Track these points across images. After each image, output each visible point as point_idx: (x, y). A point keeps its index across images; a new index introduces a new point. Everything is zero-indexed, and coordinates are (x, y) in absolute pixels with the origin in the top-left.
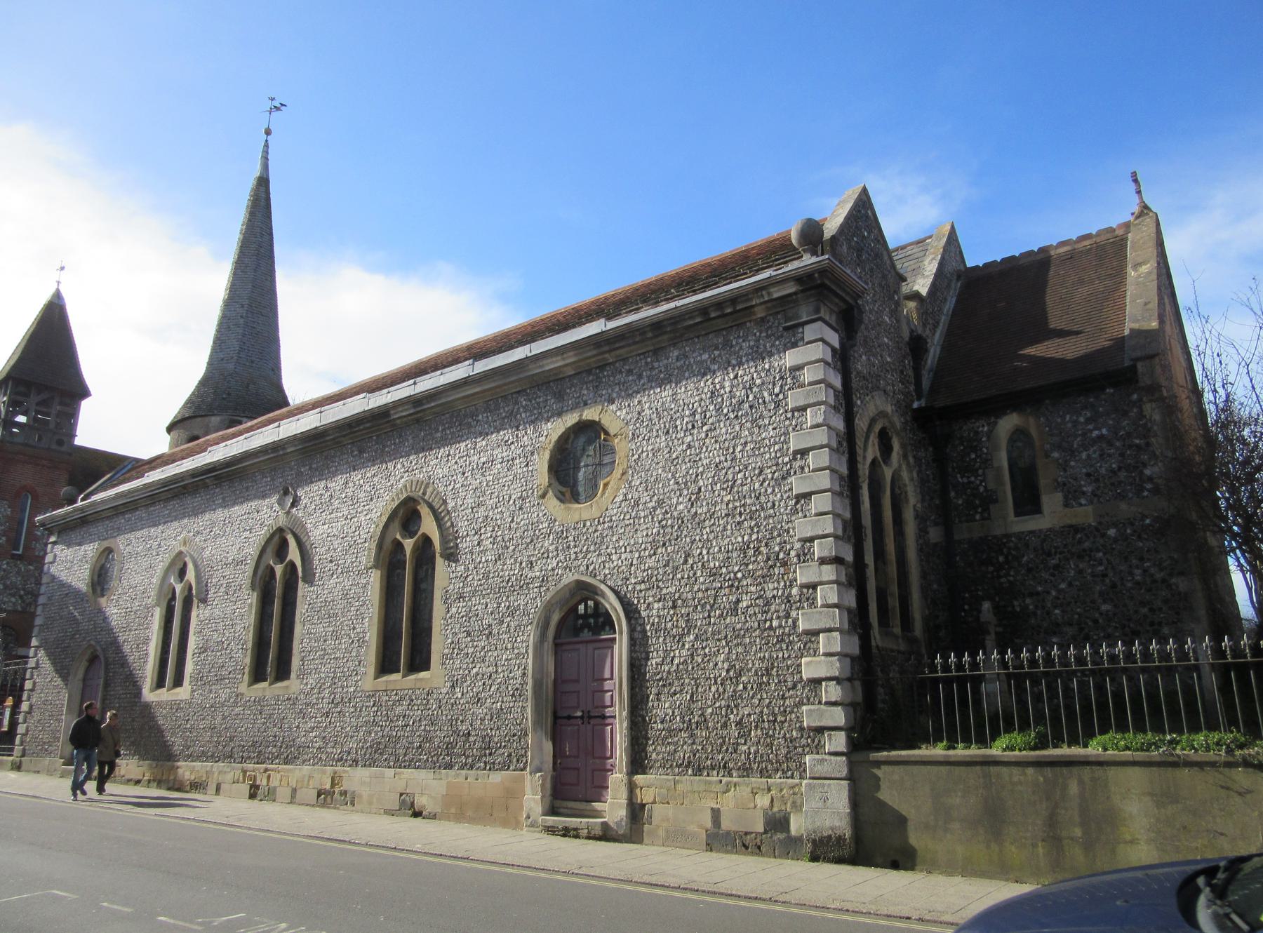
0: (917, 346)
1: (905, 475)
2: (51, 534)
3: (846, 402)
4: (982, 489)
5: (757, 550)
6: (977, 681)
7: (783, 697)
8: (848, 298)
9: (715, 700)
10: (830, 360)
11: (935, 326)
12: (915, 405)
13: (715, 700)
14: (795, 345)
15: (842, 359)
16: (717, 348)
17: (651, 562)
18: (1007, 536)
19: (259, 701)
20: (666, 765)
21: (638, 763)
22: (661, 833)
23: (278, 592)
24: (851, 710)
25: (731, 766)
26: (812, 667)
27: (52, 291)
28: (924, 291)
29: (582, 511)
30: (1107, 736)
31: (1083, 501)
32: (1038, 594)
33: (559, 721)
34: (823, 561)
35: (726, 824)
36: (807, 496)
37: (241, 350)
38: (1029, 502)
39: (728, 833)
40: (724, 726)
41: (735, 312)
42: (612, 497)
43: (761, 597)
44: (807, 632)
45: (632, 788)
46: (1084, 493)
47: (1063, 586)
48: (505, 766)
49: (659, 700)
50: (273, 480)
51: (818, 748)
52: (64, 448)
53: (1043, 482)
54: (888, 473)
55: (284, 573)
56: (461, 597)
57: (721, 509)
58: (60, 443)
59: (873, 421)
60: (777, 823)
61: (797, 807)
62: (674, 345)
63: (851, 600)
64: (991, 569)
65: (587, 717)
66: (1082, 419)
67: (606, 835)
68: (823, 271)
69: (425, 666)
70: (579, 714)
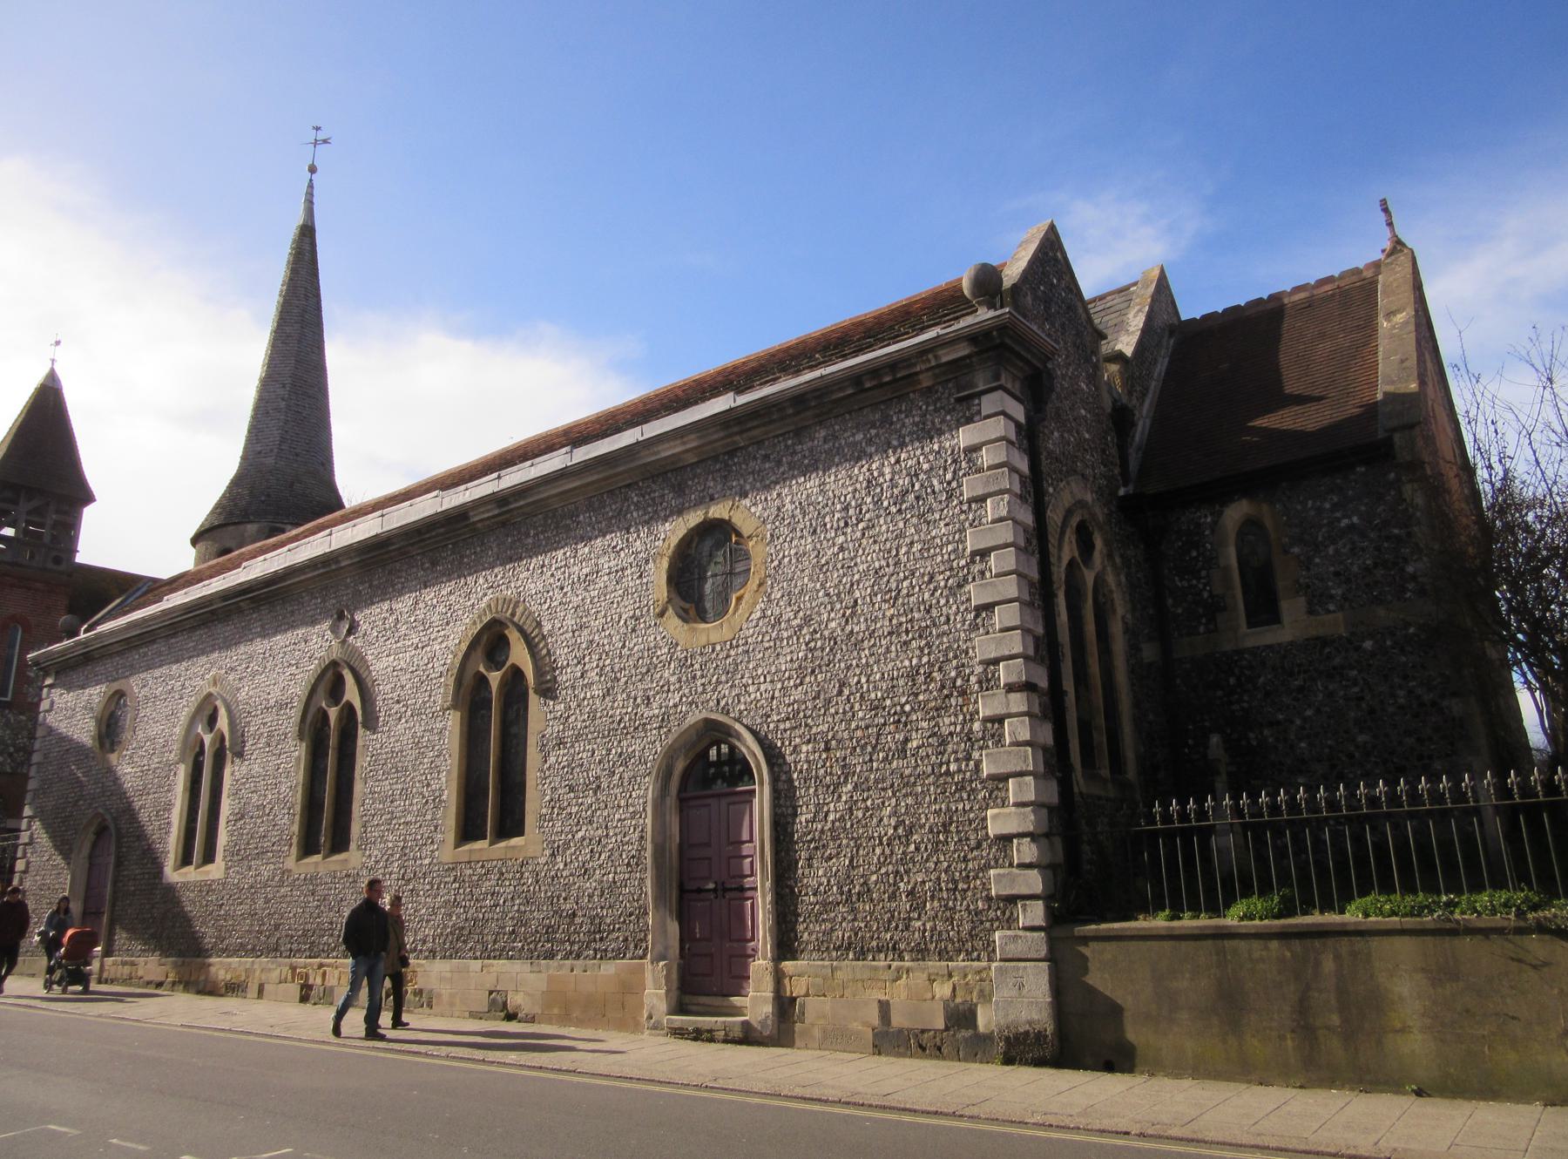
0: (1121, 419)
1: (1111, 579)
2: (47, 675)
3: (1034, 490)
4: (1206, 595)
5: (929, 676)
6: (1206, 833)
7: (965, 860)
8: (1035, 362)
9: (881, 865)
10: (1013, 438)
11: (1144, 395)
12: (1122, 492)
13: (881, 865)
14: (969, 420)
15: (1028, 437)
16: (873, 426)
17: (797, 694)
18: (1239, 652)
19: (312, 879)
20: (822, 948)
21: (786, 947)
22: (817, 1033)
23: (333, 741)
24: (1049, 873)
25: (902, 946)
26: (999, 821)
27: (46, 370)
28: (1129, 352)
29: (710, 632)
30: (1368, 899)
31: (1332, 607)
32: (1278, 723)
34: (1010, 688)
35: (898, 1020)
36: (989, 607)
37: (283, 440)
38: (1264, 609)
39: (900, 1031)
40: (893, 897)
41: (895, 380)
42: (747, 615)
43: (934, 734)
44: (992, 777)
45: (779, 977)
46: (1332, 597)
47: (1309, 713)
48: (619, 954)
49: (810, 866)
50: (324, 601)
51: (1010, 922)
52: (62, 567)
53: (1281, 584)
54: (1089, 577)
55: (340, 718)
56: (561, 743)
57: (883, 626)
58: (57, 561)
59: (1069, 513)
60: (961, 1017)
61: (986, 997)
62: (820, 423)
63: (1047, 735)
64: (1220, 693)
65: (721, 890)
66: (1327, 506)
67: (748, 1037)
68: (1002, 328)
69: (519, 831)
70: (711, 886)
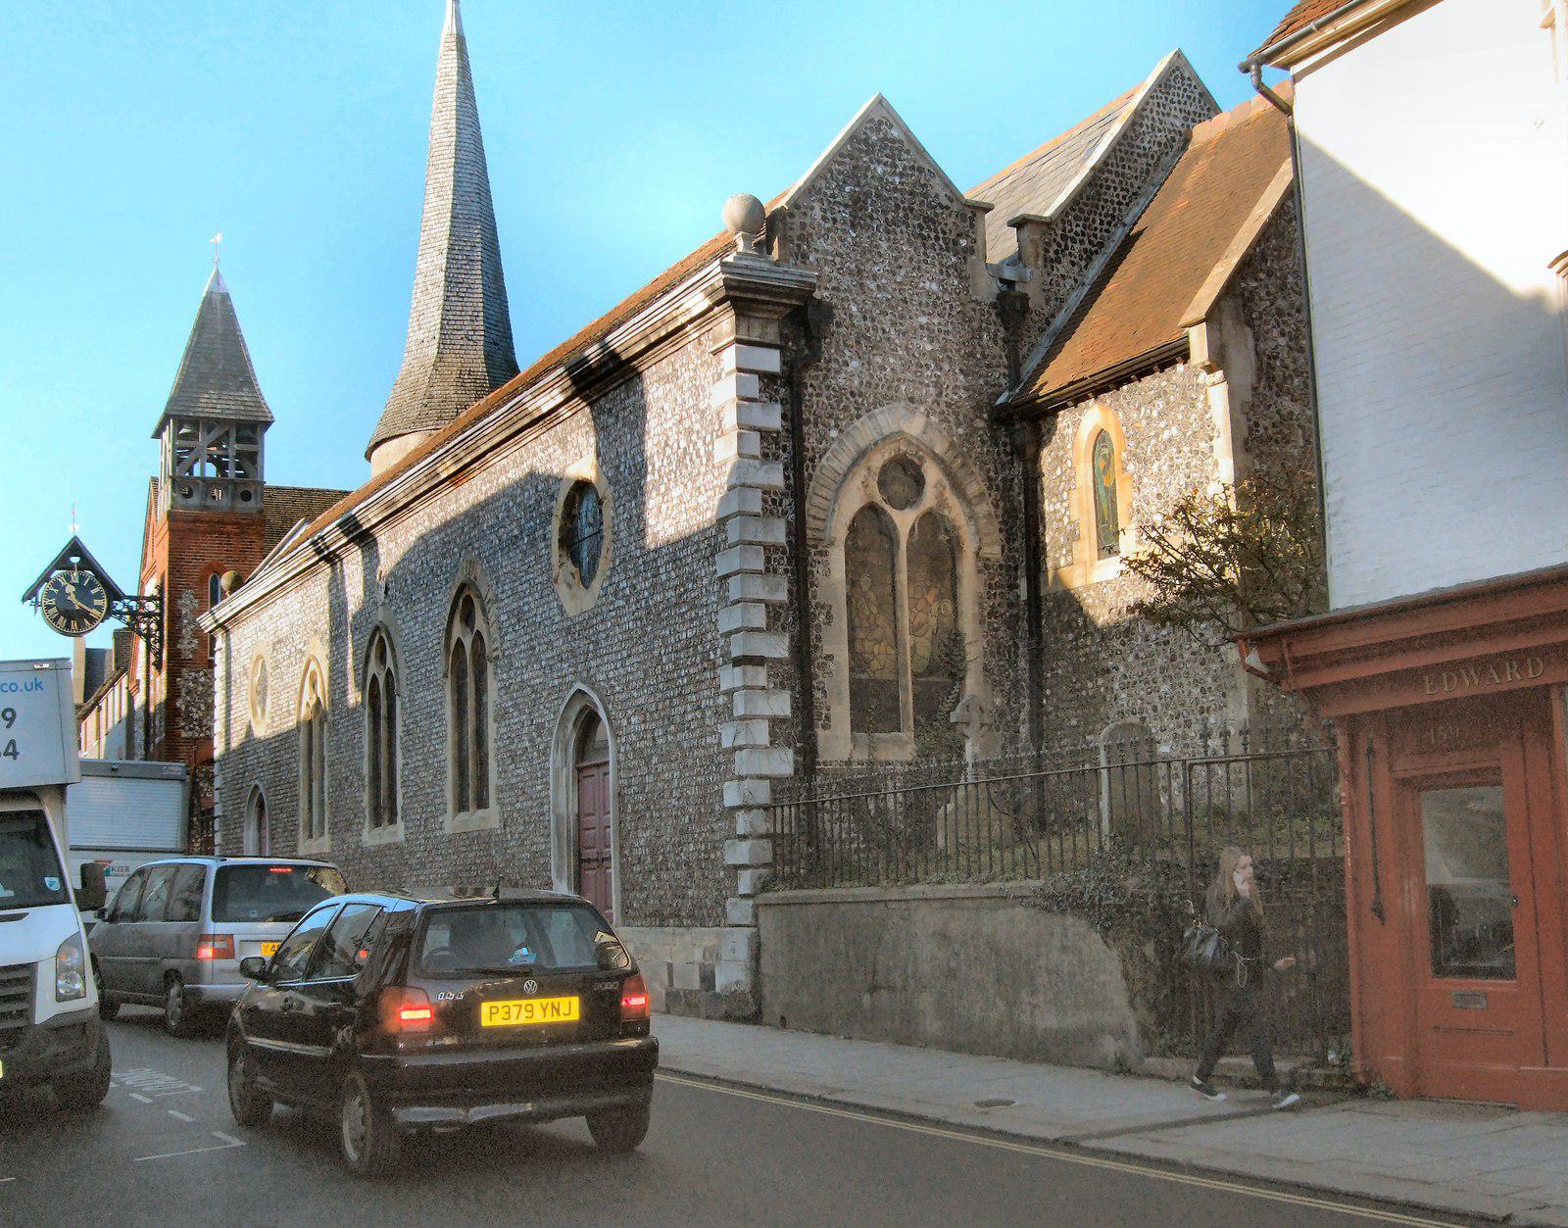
1: (956, 512)
4: (1066, 520)
12: (1001, 400)
14: (719, 378)
23: (383, 711)
25: (683, 914)
33: (585, 865)
35: (677, 985)
54: (904, 521)
59: (863, 454)
60: (708, 979)
66: (1155, 414)
69: (482, 803)
